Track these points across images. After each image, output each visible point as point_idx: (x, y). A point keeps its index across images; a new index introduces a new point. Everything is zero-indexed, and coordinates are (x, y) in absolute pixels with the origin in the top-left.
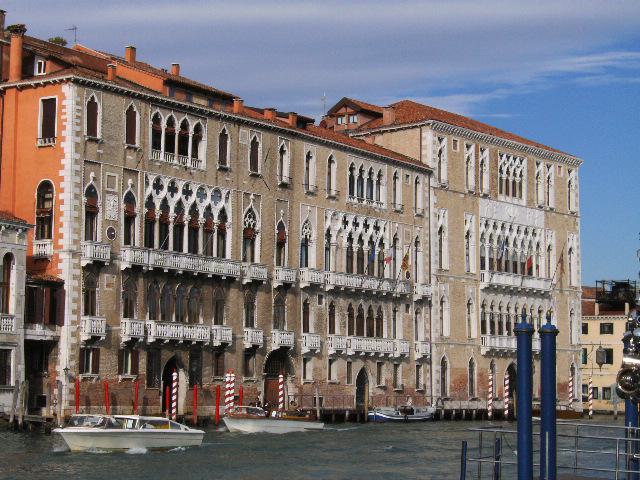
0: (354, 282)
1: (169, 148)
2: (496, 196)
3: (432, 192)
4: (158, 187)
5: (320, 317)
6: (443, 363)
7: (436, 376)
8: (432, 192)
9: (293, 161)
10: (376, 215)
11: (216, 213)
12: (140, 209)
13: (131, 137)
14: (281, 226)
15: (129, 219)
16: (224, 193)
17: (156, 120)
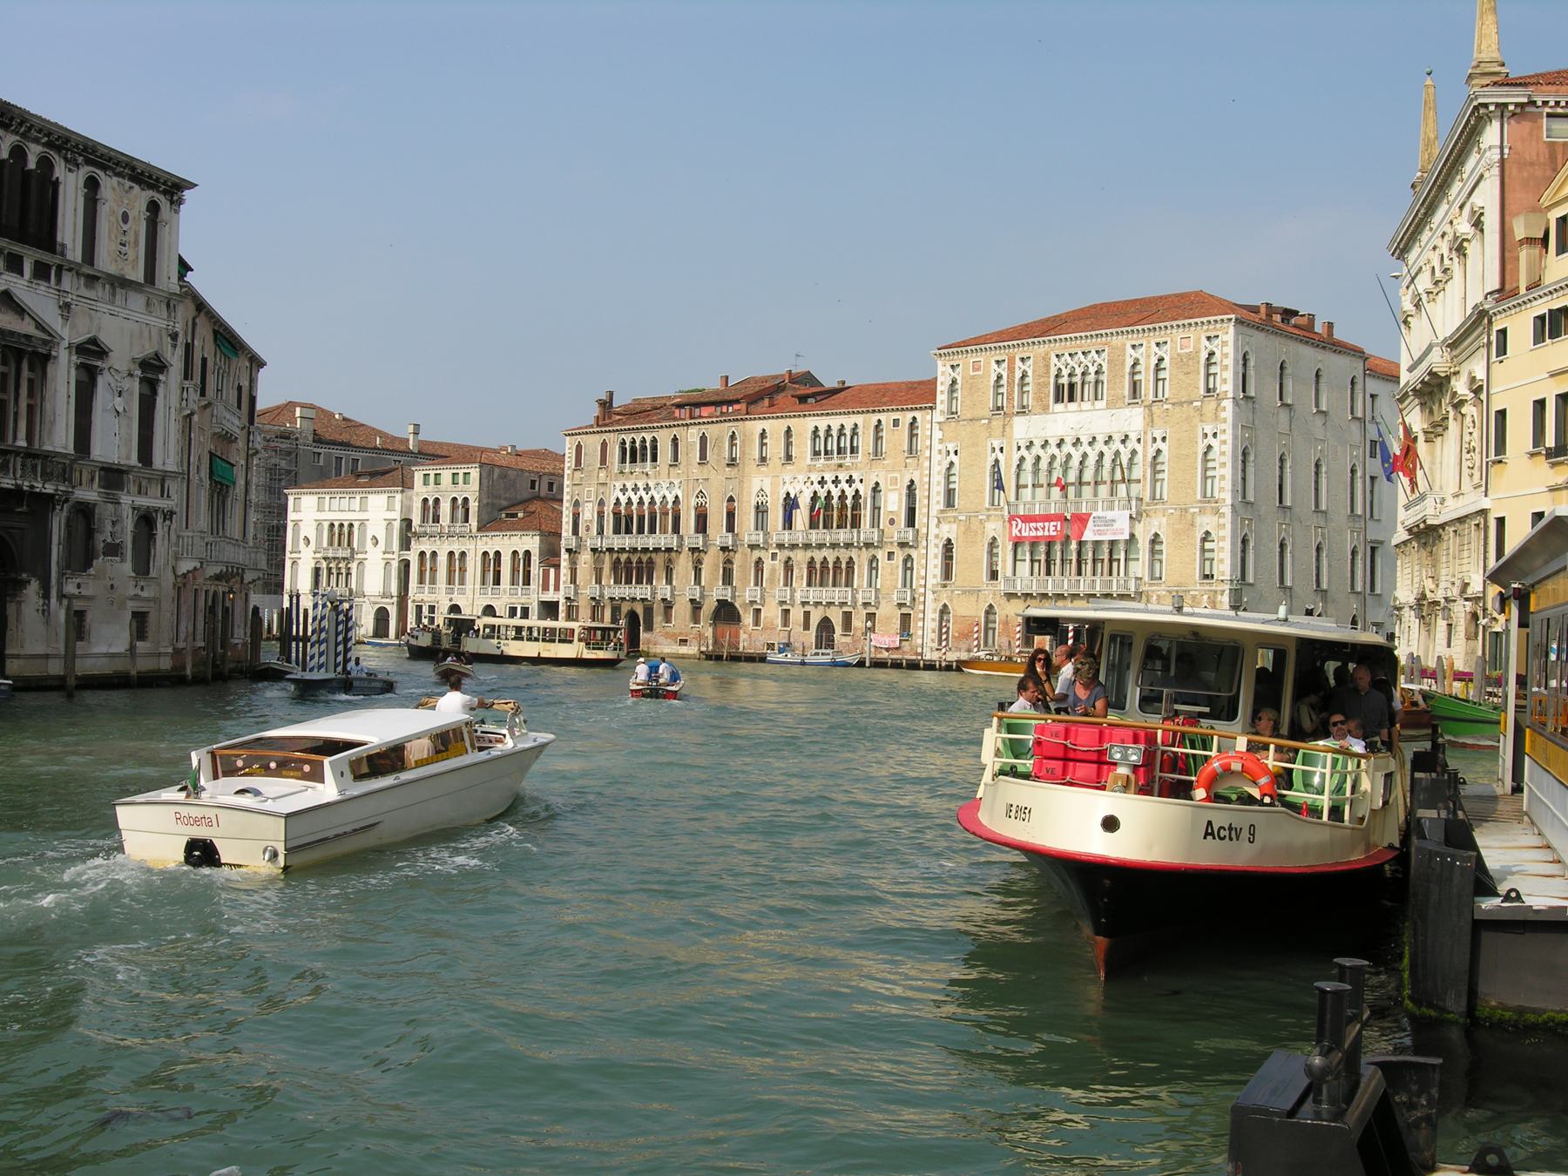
0: (815, 536)
1: (633, 460)
2: (1045, 409)
3: (936, 427)
4: (624, 490)
5: (773, 570)
6: (944, 610)
7: (931, 623)
8: (936, 427)
9: (743, 442)
10: (848, 468)
11: (670, 499)
12: (608, 509)
13: (603, 461)
14: (731, 499)
15: (601, 515)
16: (676, 482)
17: (624, 442)
